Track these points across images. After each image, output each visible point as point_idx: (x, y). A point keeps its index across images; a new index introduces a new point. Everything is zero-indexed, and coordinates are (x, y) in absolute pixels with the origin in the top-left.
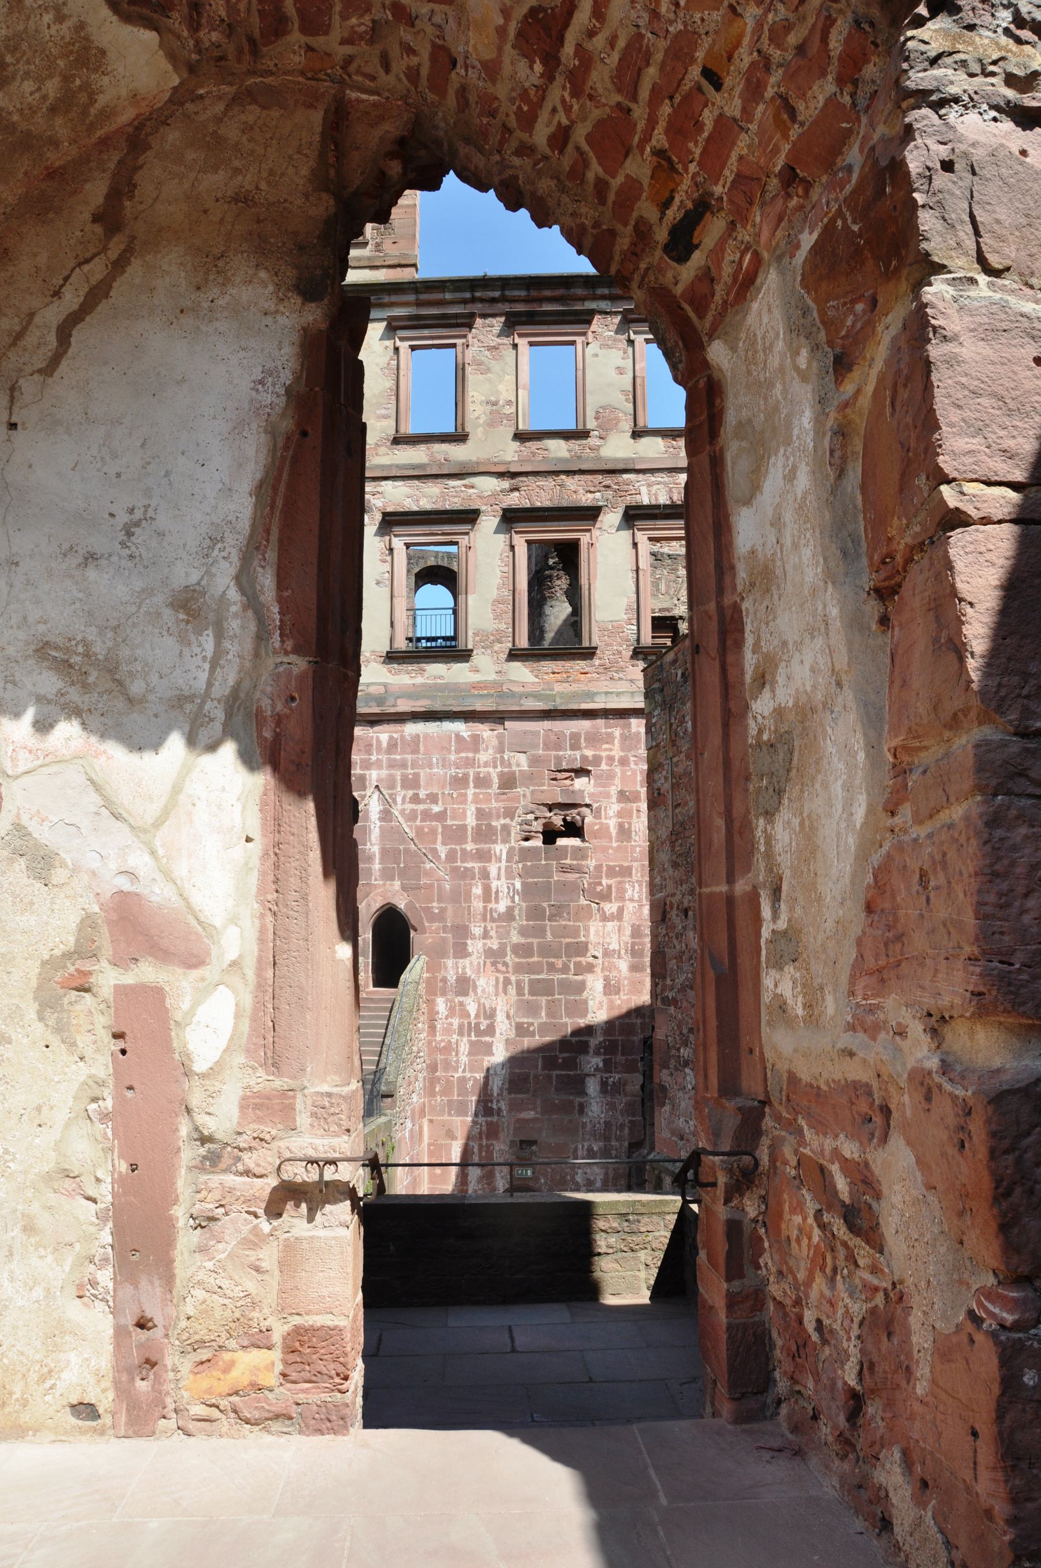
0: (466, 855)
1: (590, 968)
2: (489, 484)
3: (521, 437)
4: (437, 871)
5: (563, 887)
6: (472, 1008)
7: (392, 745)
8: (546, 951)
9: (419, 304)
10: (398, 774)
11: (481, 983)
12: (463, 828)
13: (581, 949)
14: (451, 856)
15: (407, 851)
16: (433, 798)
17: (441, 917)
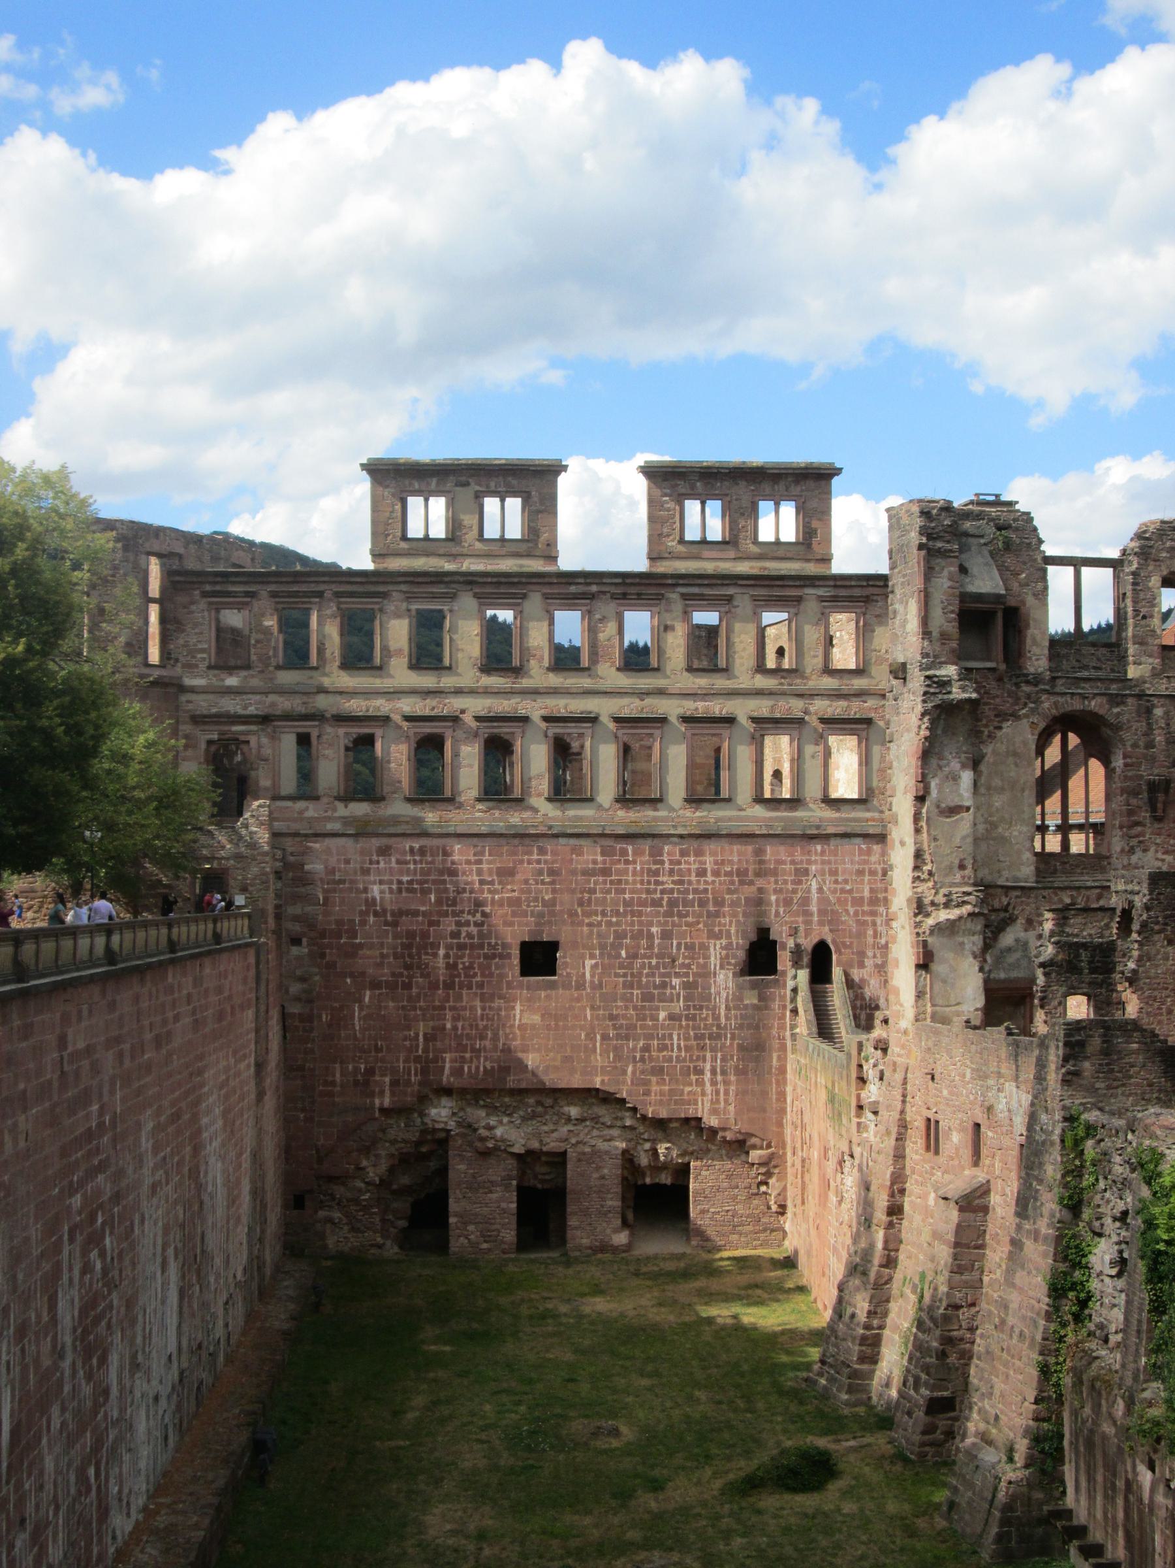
0: (864, 913)
4: (849, 923)
9: (835, 586)
10: (827, 868)
11: (872, 982)
12: (862, 898)
14: (856, 913)
15: (832, 910)
16: (846, 881)
17: (850, 946)
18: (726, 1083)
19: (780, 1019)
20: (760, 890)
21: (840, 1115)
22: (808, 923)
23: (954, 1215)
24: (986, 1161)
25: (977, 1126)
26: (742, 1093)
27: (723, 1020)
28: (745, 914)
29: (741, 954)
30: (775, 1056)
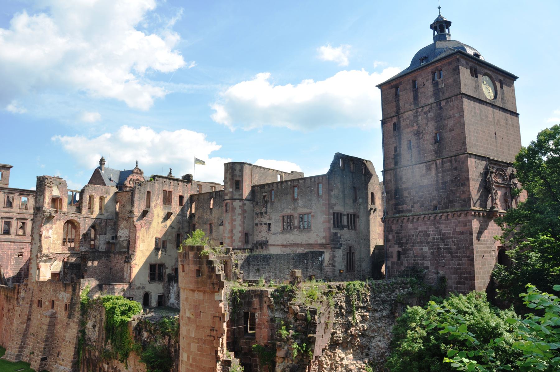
3: (20, 209)
21: (10, 300)
23: (49, 319)
24: (55, 308)
25: (53, 301)
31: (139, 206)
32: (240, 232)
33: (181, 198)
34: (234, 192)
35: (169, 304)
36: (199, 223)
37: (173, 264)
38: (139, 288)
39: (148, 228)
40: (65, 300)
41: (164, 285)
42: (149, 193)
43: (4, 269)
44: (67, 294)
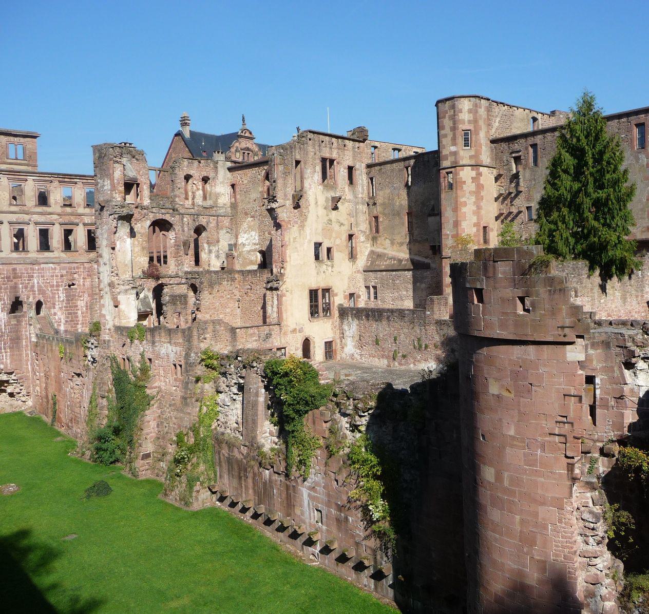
0: (54, 290)
1: (78, 310)
2: (55, 217)
5: (73, 295)
6: (57, 318)
7: (39, 269)
8: (70, 307)
11: (58, 313)
13: (77, 306)
14: (52, 290)
16: (47, 279)
18: (6, 352)
19: (25, 328)
20: (15, 283)
22: (35, 294)
26: (12, 355)
27: (3, 330)
28: (10, 292)
29: (9, 307)
30: (24, 341)
31: (285, 185)
32: (475, 225)
33: (350, 169)
34: (462, 153)
35: (344, 355)
36: (384, 214)
37: (346, 287)
38: (294, 331)
39: (302, 227)
40: (172, 355)
41: (333, 324)
42: (298, 163)
43: (50, 308)
44: (174, 349)
